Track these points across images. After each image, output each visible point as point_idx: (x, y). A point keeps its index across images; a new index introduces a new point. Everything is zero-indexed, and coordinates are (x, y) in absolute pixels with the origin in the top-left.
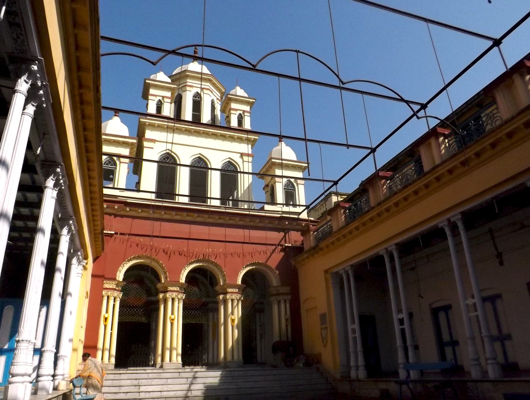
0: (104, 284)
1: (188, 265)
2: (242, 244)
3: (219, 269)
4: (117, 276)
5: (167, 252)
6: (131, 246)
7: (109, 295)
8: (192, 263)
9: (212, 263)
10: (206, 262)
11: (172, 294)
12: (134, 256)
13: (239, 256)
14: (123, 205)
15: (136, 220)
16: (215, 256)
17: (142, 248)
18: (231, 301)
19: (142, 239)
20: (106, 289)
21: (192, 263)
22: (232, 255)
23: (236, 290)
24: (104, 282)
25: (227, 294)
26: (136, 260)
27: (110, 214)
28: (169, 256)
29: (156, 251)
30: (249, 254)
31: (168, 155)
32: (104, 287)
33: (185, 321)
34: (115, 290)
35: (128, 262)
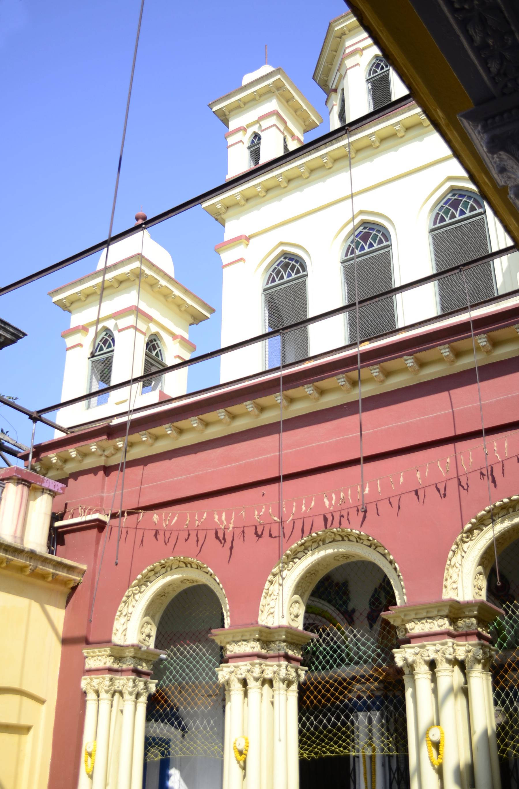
0: (87, 660)
1: (287, 563)
2: (450, 447)
3: (384, 555)
4: (114, 631)
5: (224, 534)
6: (142, 540)
7: (97, 688)
8: (299, 555)
9: (359, 538)
10: (343, 540)
11: (235, 667)
12: (149, 568)
13: (442, 492)
14: (105, 437)
15: (152, 468)
16: (361, 514)
17: (167, 541)
18: (426, 668)
19: (155, 516)
20: (90, 671)
21: (295, 556)
22: (416, 492)
23: (439, 626)
24: (85, 652)
25: (409, 642)
26: (163, 578)
27: (94, 471)
28: (230, 545)
29: (198, 541)
30: (482, 474)
31: (285, 258)
32: (87, 667)
33: (328, 750)
34: (110, 670)
35: (144, 587)
